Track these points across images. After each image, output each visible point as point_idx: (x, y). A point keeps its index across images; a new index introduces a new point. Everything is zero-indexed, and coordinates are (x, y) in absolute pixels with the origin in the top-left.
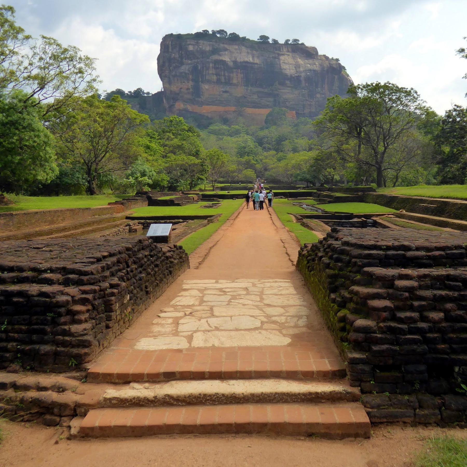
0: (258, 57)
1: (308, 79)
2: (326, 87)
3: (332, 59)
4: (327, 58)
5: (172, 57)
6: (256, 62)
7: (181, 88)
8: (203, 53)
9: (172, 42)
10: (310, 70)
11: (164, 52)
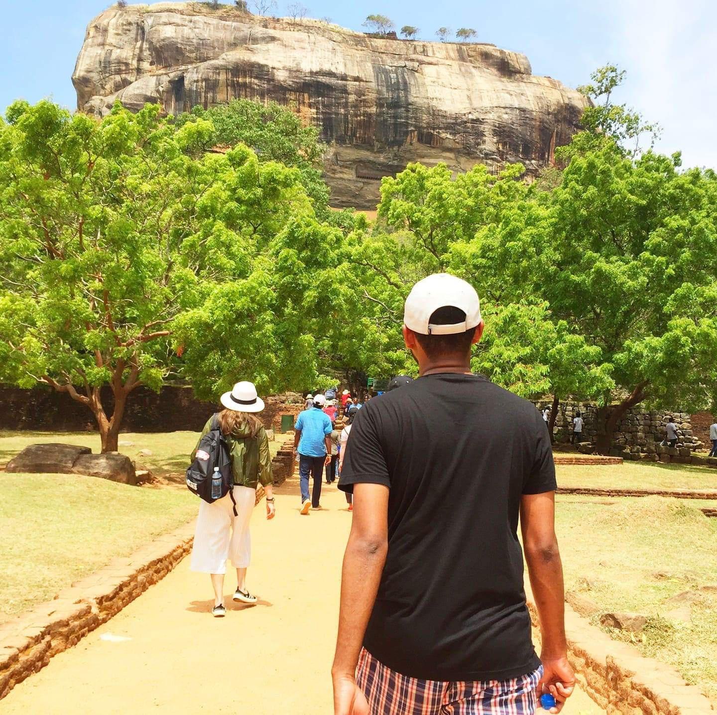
1: (502, 132)
8: (203, 44)
10: (512, 108)
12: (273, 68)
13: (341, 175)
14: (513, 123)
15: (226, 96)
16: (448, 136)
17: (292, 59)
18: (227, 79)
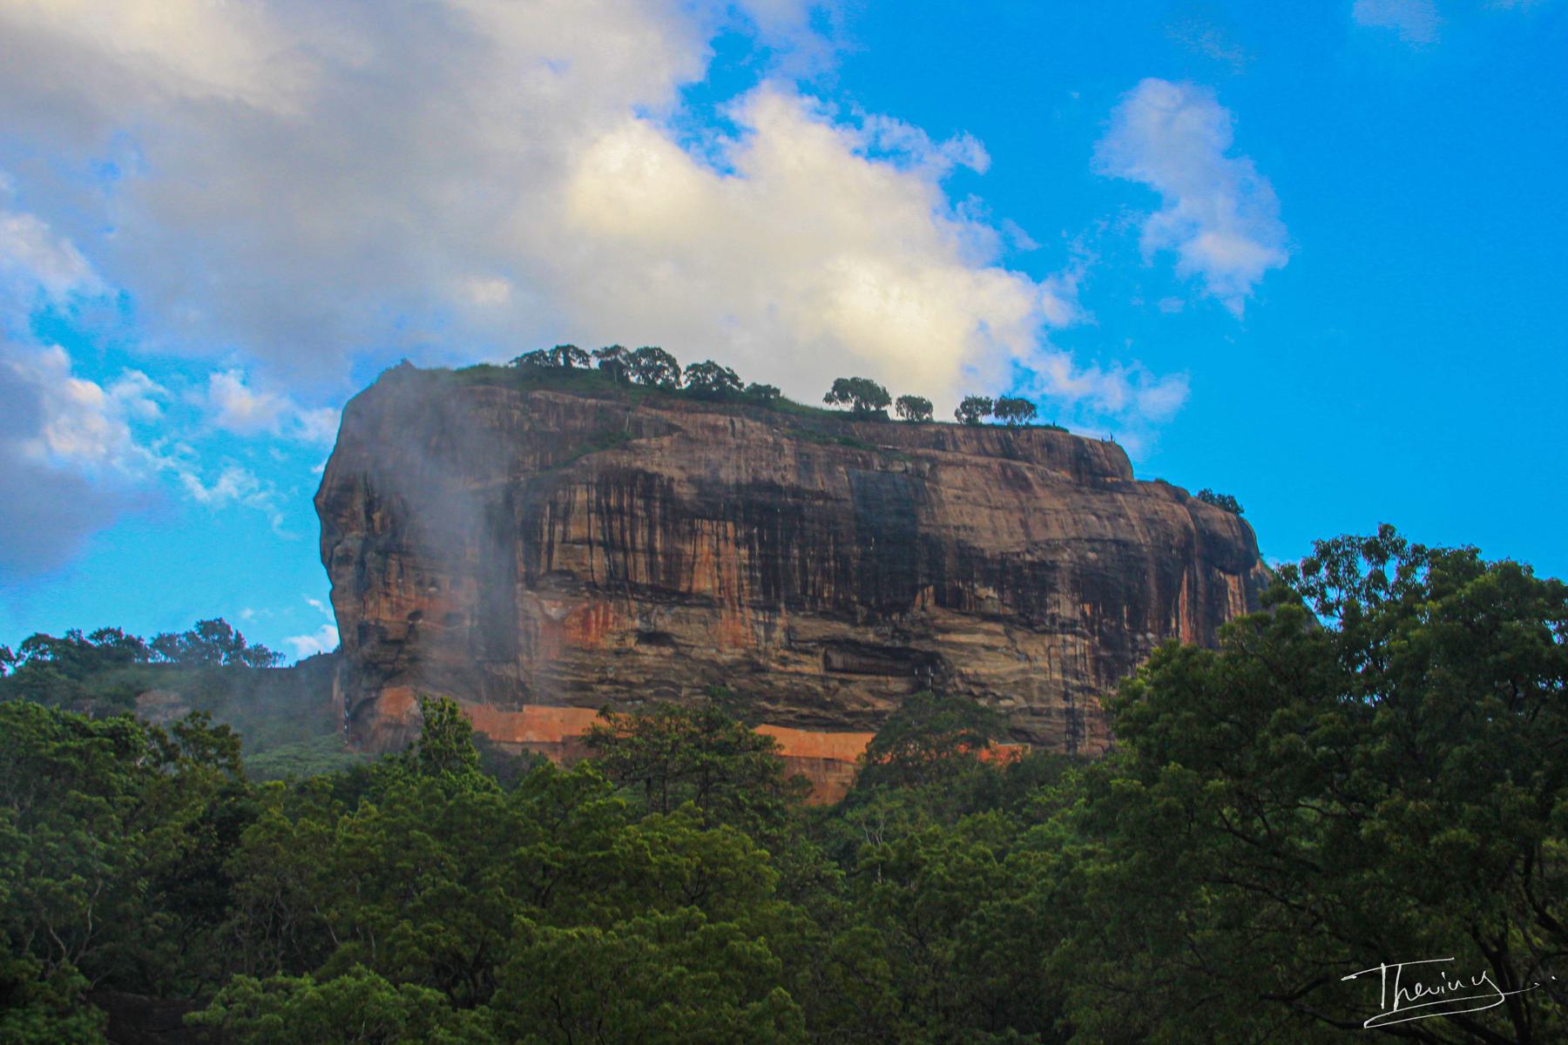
0: (830, 471)
1: (1088, 584)
3: (1205, 496)
4: (1179, 496)
7: (416, 615)
12: (671, 480)
13: (799, 668)
14: (1106, 568)
16: (991, 592)
18: (589, 501)
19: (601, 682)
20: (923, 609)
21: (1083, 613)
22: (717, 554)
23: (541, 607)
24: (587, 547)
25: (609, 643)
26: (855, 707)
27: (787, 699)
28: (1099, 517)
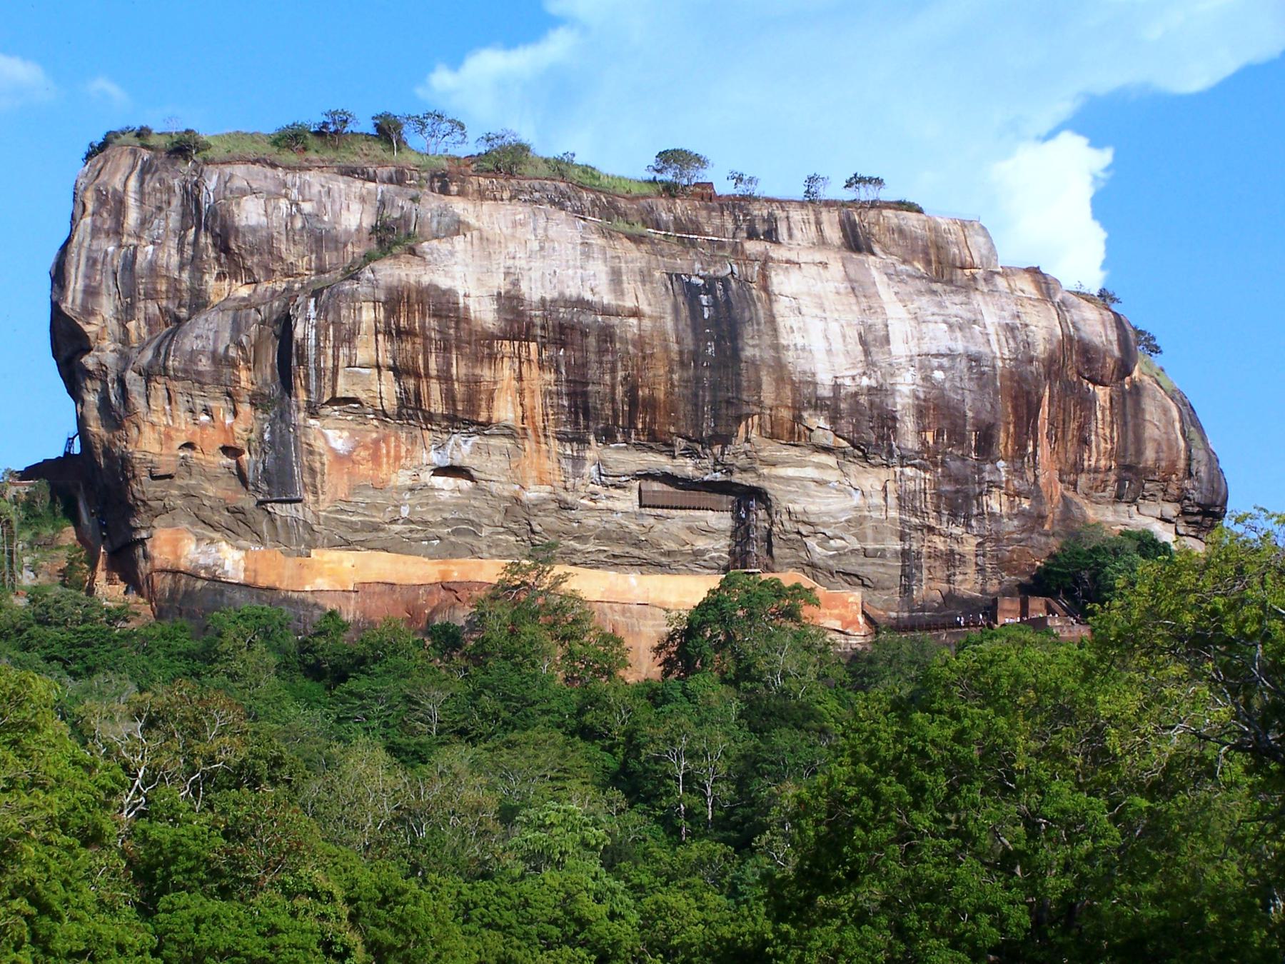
0: (645, 277)
1: (934, 408)
2: (1044, 452)
5: (140, 257)
6: (629, 303)
8: (320, 239)
9: (142, 182)
10: (951, 355)
11: (95, 231)
15: (374, 353)
16: (822, 423)
17: (502, 270)
18: (376, 321)
19: (394, 521)
20: (747, 440)
21: (924, 443)
22: (520, 378)
23: (327, 441)
24: (376, 371)
25: (402, 478)
26: (674, 546)
27: (597, 538)
28: (950, 326)
